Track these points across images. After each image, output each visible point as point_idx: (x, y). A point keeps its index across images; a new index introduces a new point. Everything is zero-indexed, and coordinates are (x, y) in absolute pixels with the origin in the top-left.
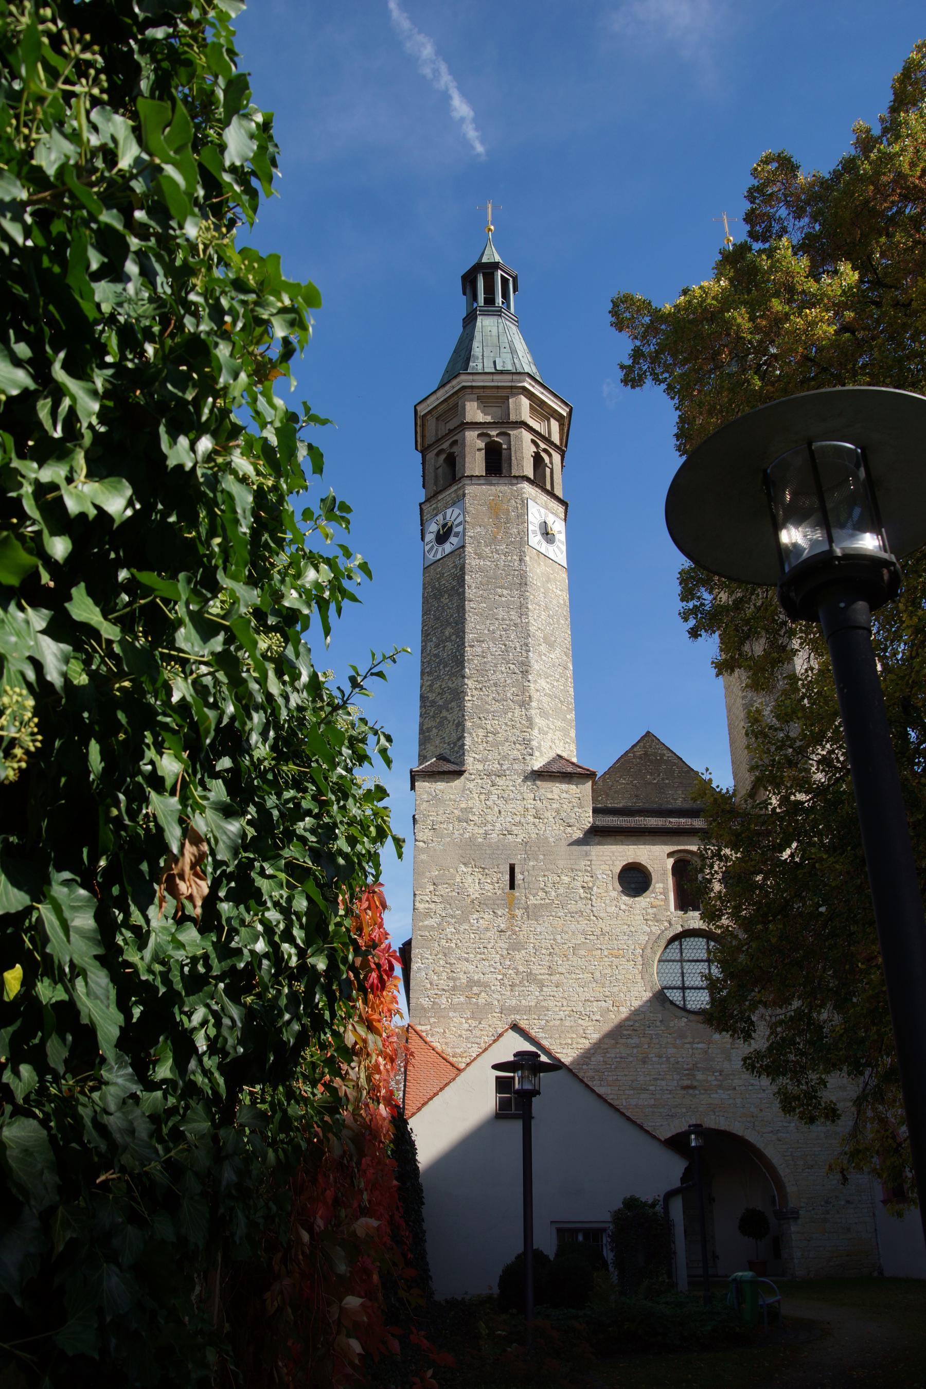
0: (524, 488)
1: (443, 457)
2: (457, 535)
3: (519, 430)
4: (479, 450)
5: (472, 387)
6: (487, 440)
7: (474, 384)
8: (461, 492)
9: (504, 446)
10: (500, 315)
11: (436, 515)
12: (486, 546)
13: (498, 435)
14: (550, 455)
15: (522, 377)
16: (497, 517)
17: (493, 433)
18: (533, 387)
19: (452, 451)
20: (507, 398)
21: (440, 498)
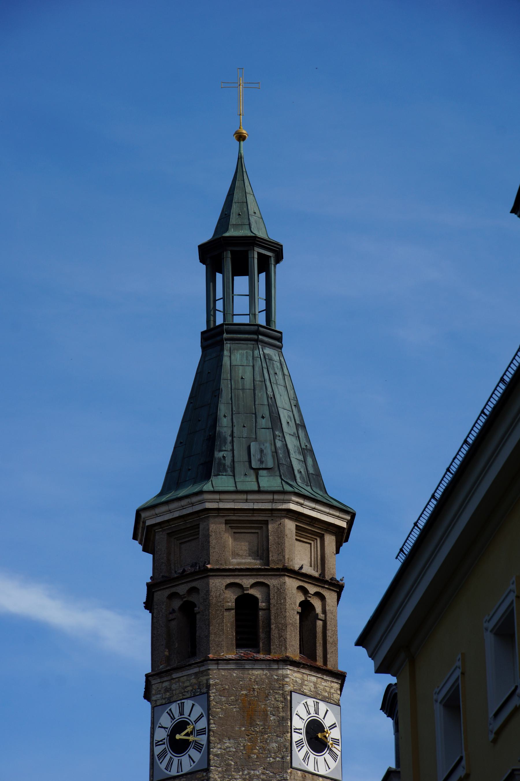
0: (286, 676)
1: (177, 604)
2: (198, 747)
3: (282, 579)
4: (228, 610)
5: (218, 510)
6: (239, 593)
7: (222, 505)
8: (203, 679)
9: (262, 605)
10: (257, 341)
11: (171, 702)
12: (237, 771)
13: (253, 586)
14: (322, 598)
15: (287, 497)
16: (252, 723)
17: (247, 582)
18: (301, 505)
19: (191, 599)
20: (266, 523)
21: (174, 676)
